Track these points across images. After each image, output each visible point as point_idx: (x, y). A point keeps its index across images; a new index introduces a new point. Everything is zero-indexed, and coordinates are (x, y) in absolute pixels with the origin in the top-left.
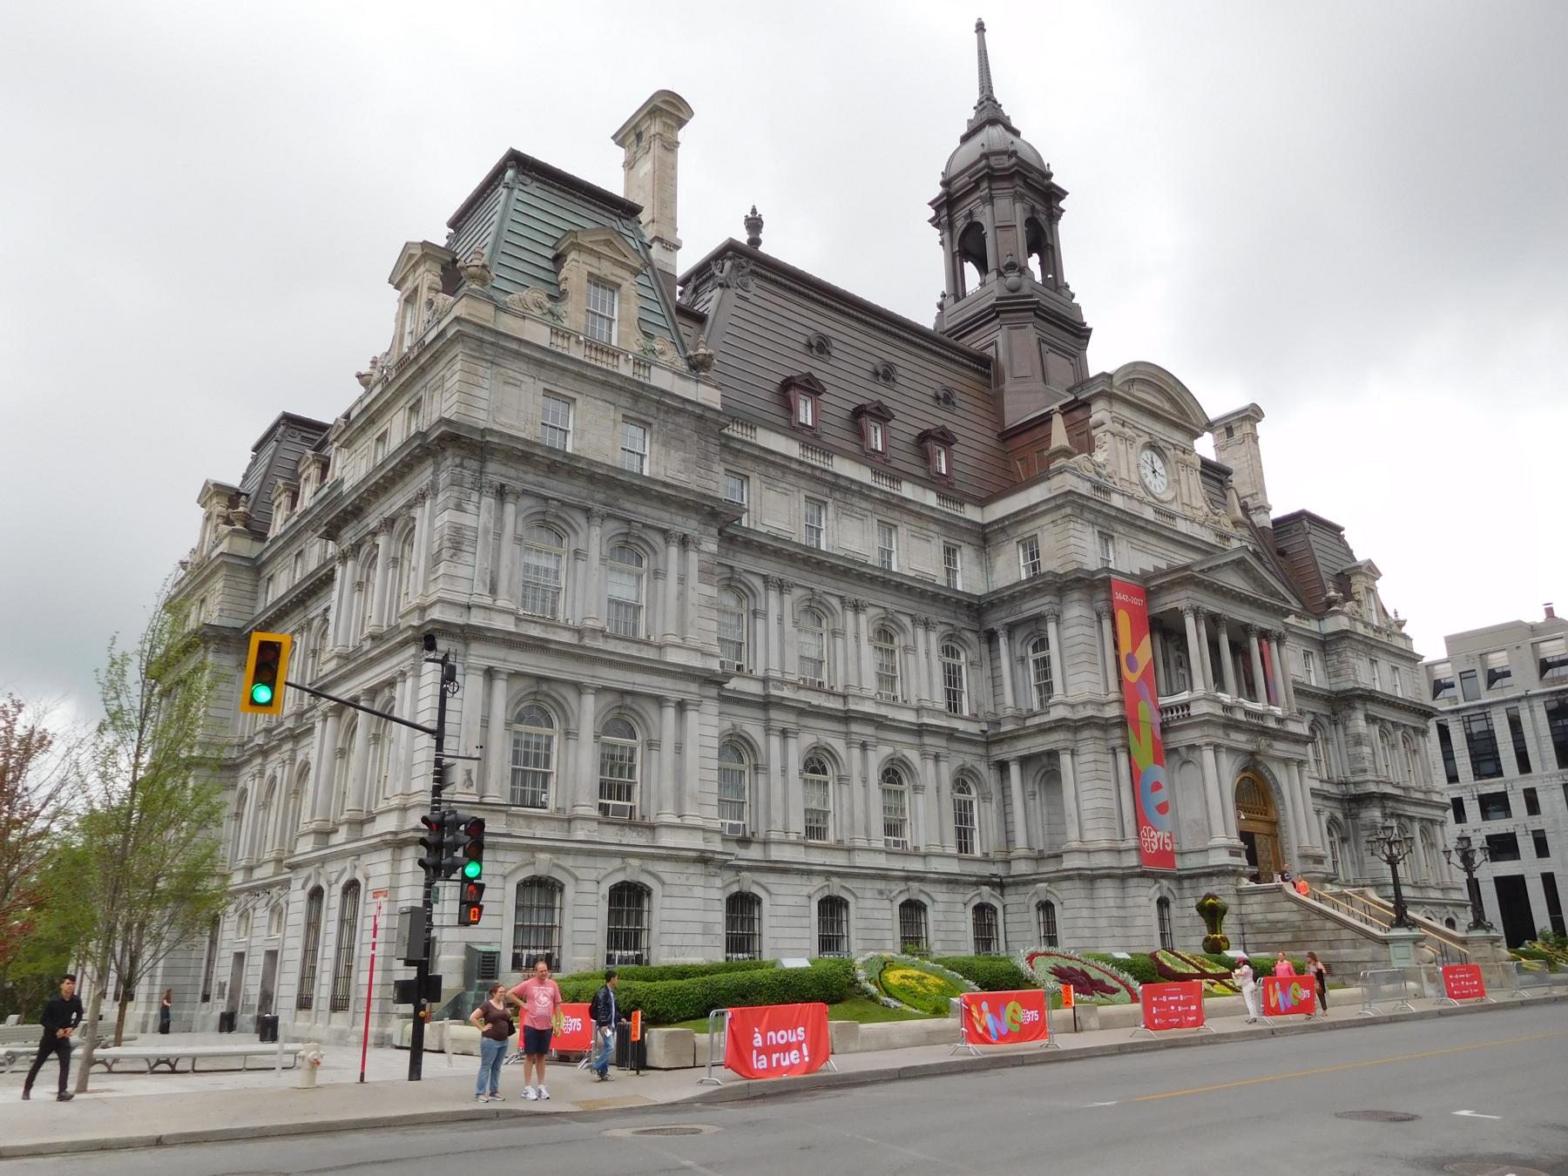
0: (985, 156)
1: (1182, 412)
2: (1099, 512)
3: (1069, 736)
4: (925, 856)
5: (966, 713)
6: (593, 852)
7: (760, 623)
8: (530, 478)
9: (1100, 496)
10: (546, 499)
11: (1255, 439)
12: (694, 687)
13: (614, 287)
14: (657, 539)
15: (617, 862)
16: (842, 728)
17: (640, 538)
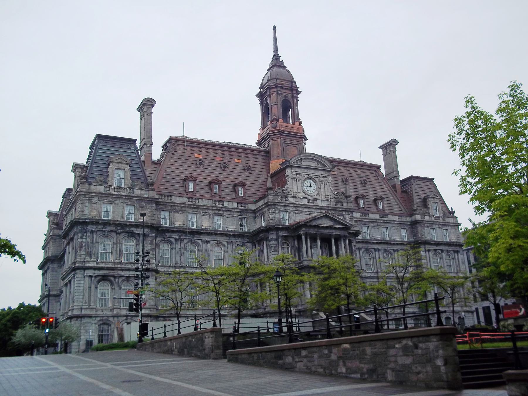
0: (268, 81)
1: (323, 164)
7: (174, 251)
8: (100, 227)
11: (395, 152)
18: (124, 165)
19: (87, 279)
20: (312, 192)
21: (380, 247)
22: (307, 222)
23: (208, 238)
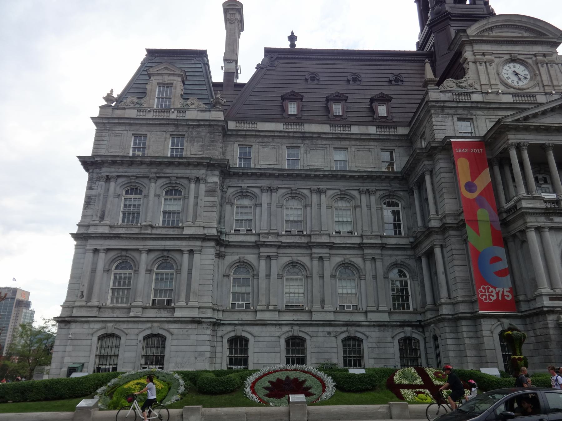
1: (540, 34)
2: (457, 107)
3: (439, 237)
4: (366, 313)
5: (403, 234)
6: (136, 321)
8: (121, 170)
9: (463, 98)
10: (129, 177)
12: (199, 243)
13: (170, 85)
14: (185, 182)
15: (149, 325)
16: (308, 251)
17: (176, 183)
18: (172, 78)
19: (90, 255)
20: (521, 84)
23: (322, 185)
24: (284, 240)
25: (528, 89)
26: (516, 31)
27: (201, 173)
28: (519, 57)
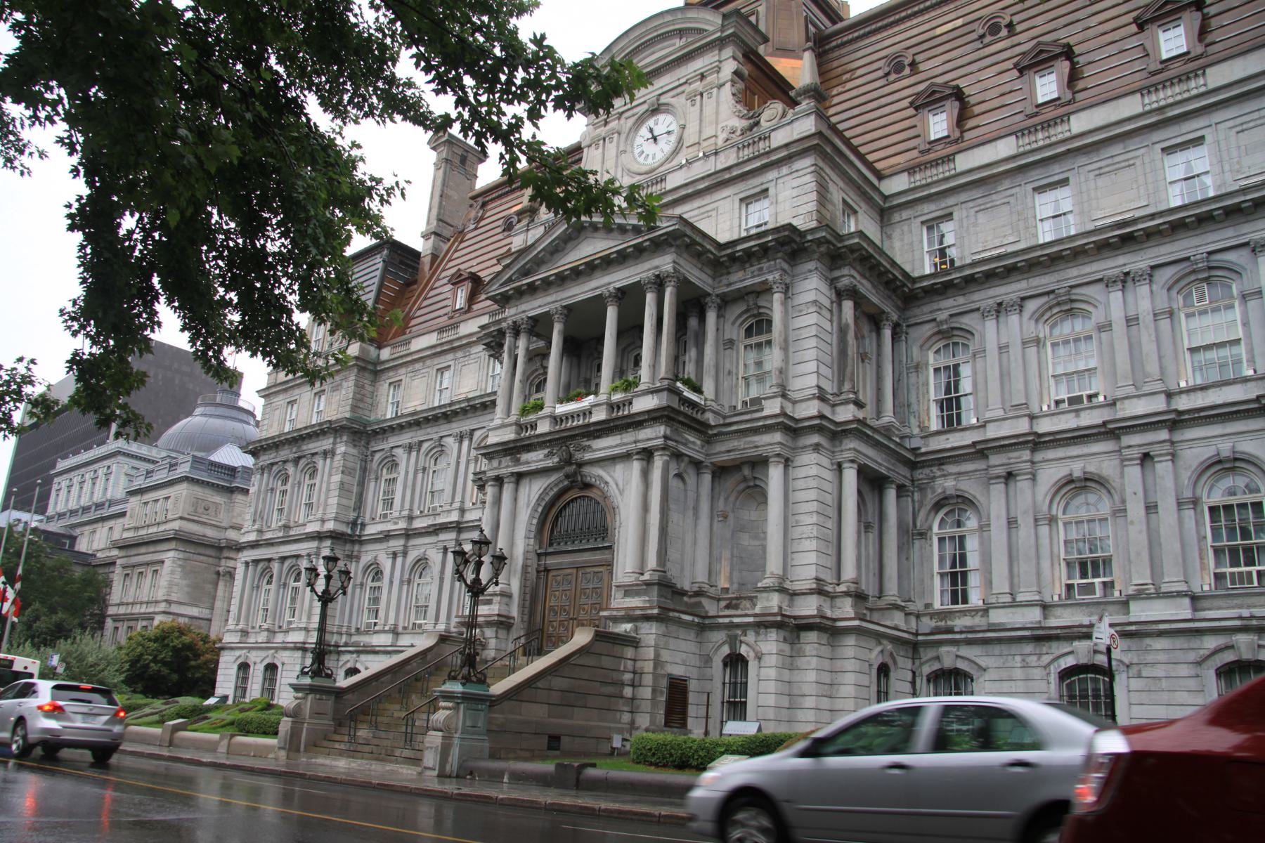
21: (1138, 261)
22: (510, 280)
24: (419, 524)
25: (662, 165)
26: (666, 44)
27: (326, 443)
28: (663, 100)
